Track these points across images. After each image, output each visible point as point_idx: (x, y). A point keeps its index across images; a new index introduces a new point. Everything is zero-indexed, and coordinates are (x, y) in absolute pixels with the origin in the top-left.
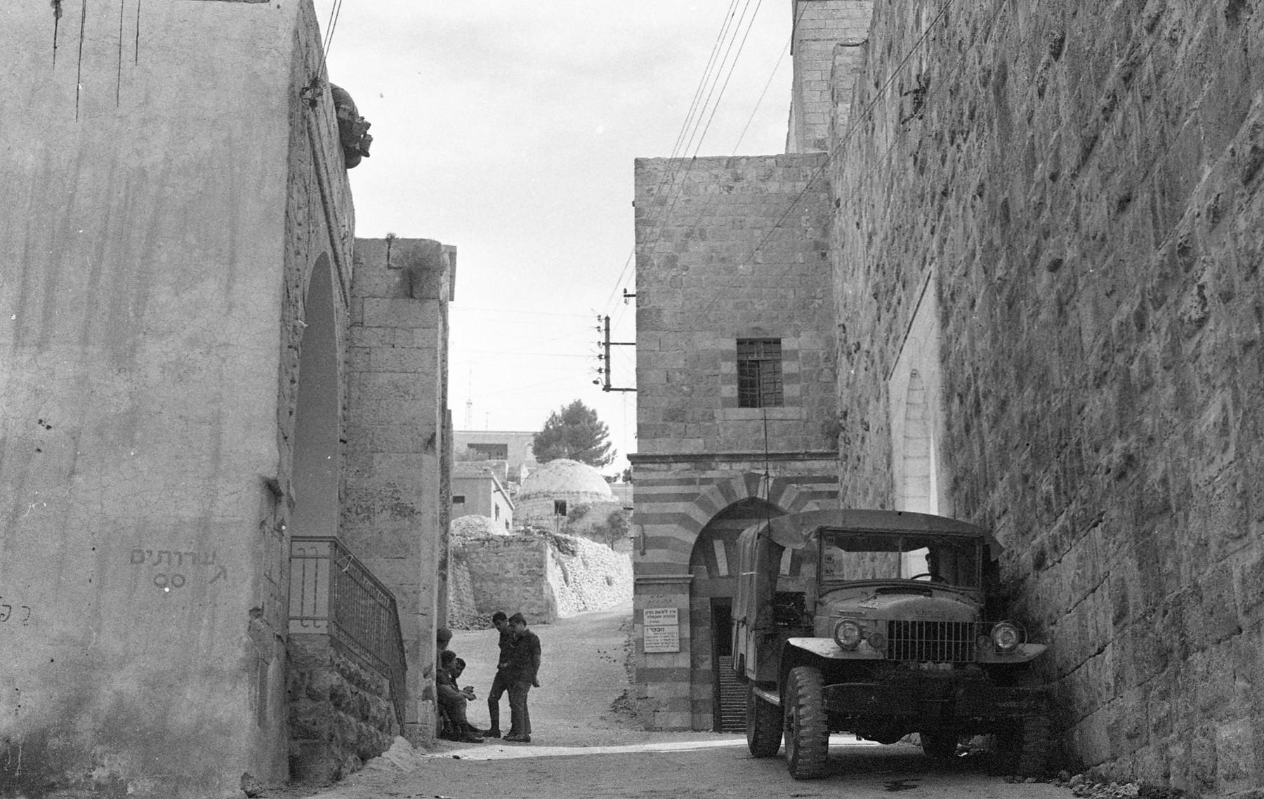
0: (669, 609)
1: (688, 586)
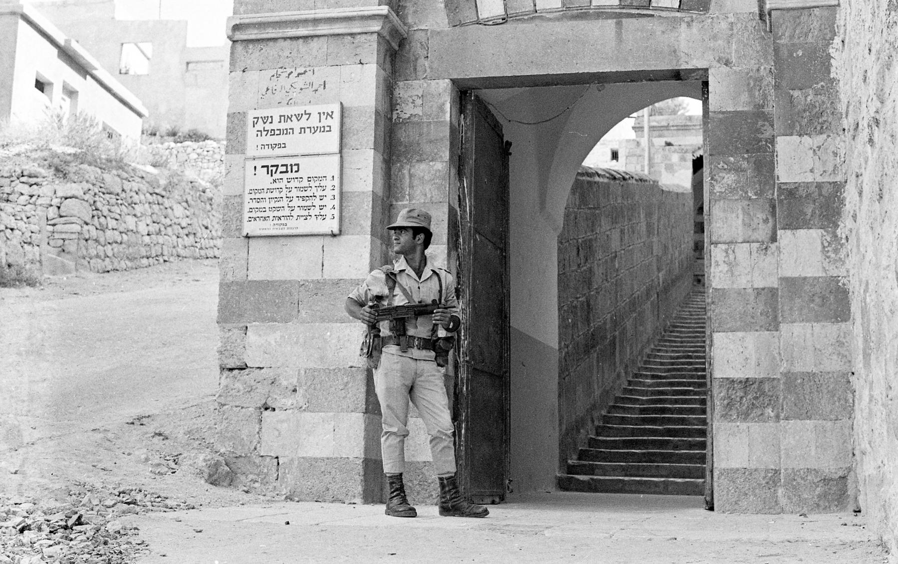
0: (314, 110)
1: (375, 36)
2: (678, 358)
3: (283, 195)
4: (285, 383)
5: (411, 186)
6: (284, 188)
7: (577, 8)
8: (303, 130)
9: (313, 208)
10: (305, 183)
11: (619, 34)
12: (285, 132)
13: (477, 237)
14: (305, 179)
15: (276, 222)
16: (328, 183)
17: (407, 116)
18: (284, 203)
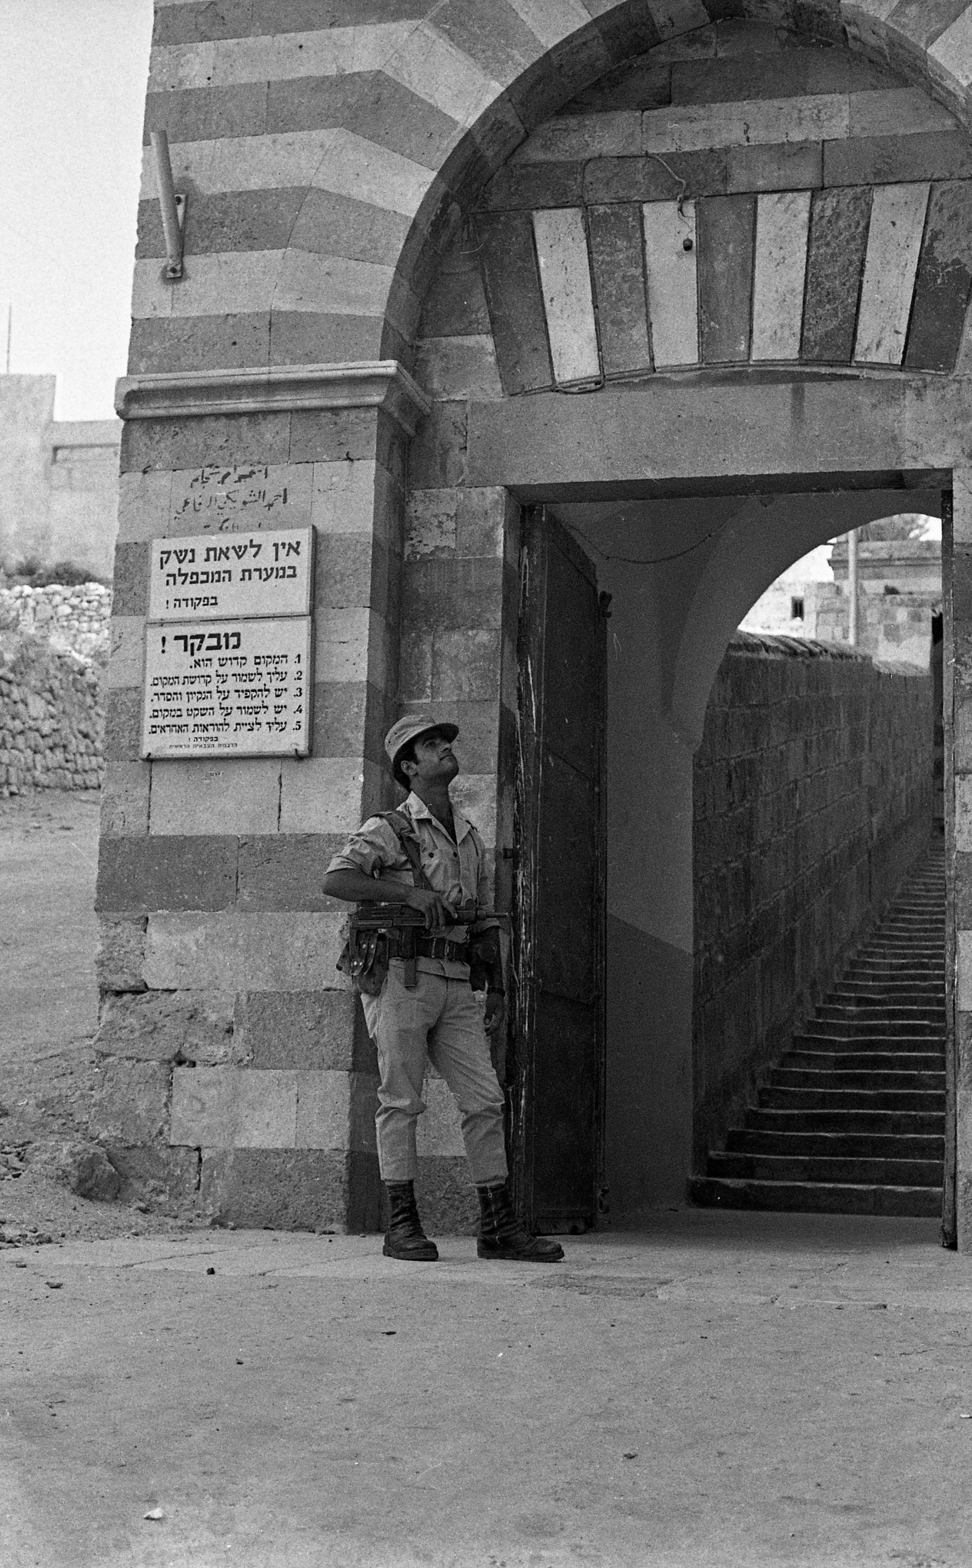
0: (266, 538)
1: (374, 413)
2: (903, 967)
3: (212, 687)
4: (213, 1017)
5: (436, 673)
6: (213, 675)
7: (725, 365)
8: (247, 574)
9: (263, 710)
10: (250, 668)
11: (797, 412)
12: (216, 577)
13: (550, 759)
14: (251, 660)
15: (200, 734)
16: (290, 668)
17: (427, 550)
18: (214, 702)
